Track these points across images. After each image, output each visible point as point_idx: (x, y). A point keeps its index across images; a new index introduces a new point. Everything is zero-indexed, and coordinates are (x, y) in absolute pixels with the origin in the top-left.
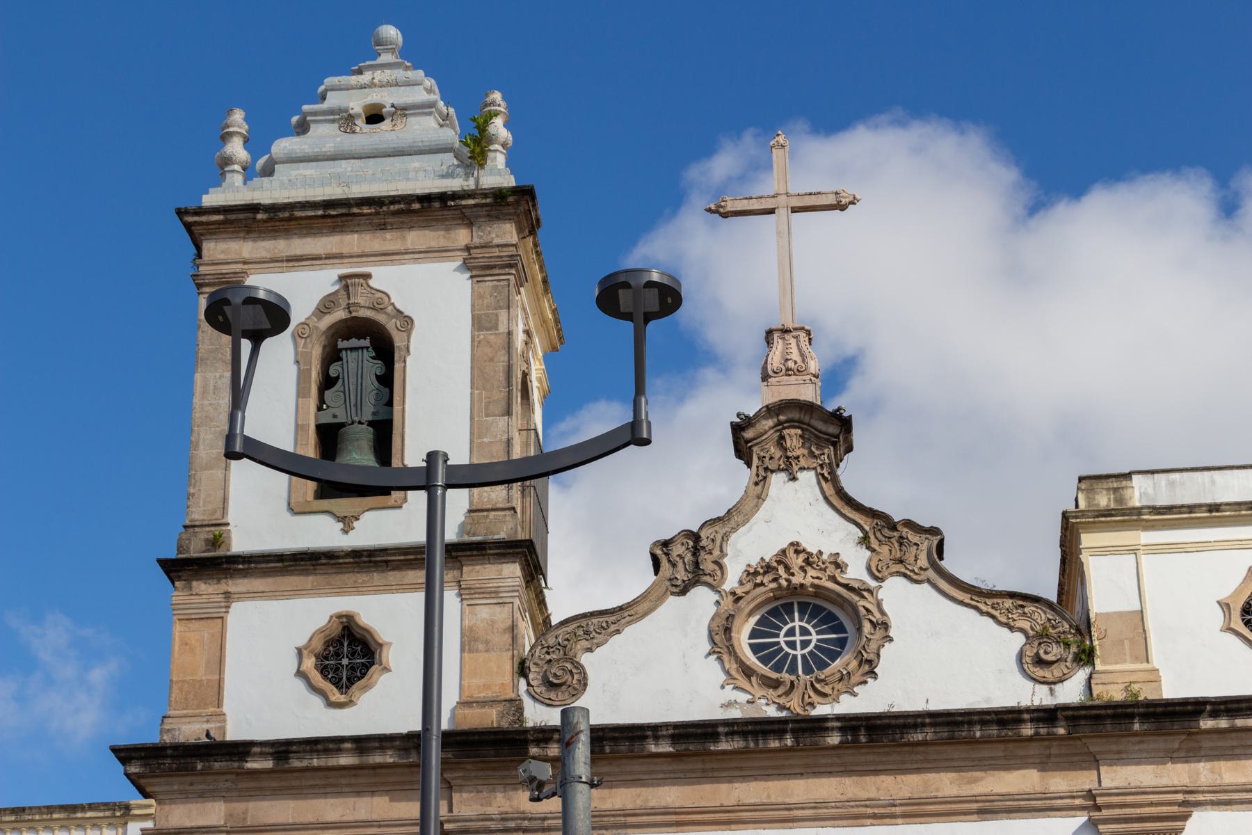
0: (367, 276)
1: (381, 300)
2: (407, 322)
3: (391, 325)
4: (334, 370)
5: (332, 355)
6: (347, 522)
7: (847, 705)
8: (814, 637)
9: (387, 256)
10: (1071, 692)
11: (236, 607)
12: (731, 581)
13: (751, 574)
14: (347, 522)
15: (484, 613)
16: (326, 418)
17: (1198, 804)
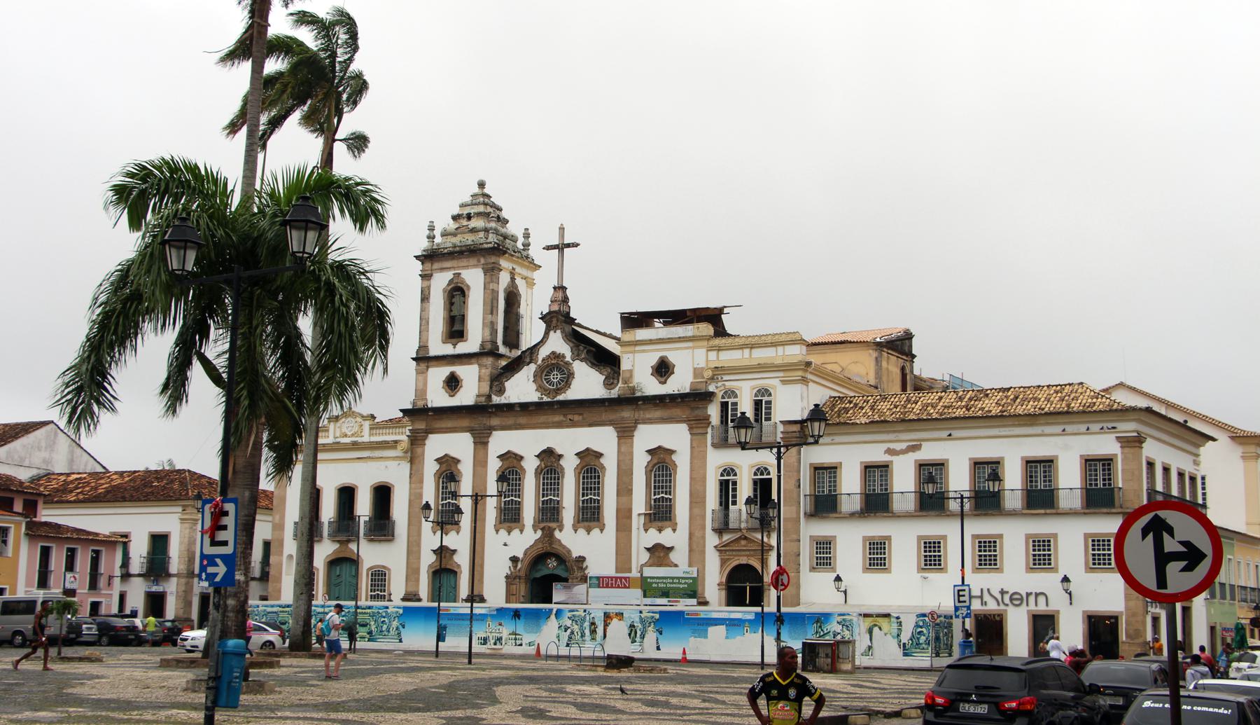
0: (460, 274)
1: (463, 282)
2: (468, 287)
3: (465, 288)
4: (454, 300)
5: (453, 297)
6: (455, 345)
7: (561, 397)
8: (559, 376)
9: (466, 267)
10: (614, 393)
11: (430, 369)
12: (540, 362)
13: (543, 360)
14: (455, 345)
15: (483, 371)
16: (452, 314)
17: (640, 423)
